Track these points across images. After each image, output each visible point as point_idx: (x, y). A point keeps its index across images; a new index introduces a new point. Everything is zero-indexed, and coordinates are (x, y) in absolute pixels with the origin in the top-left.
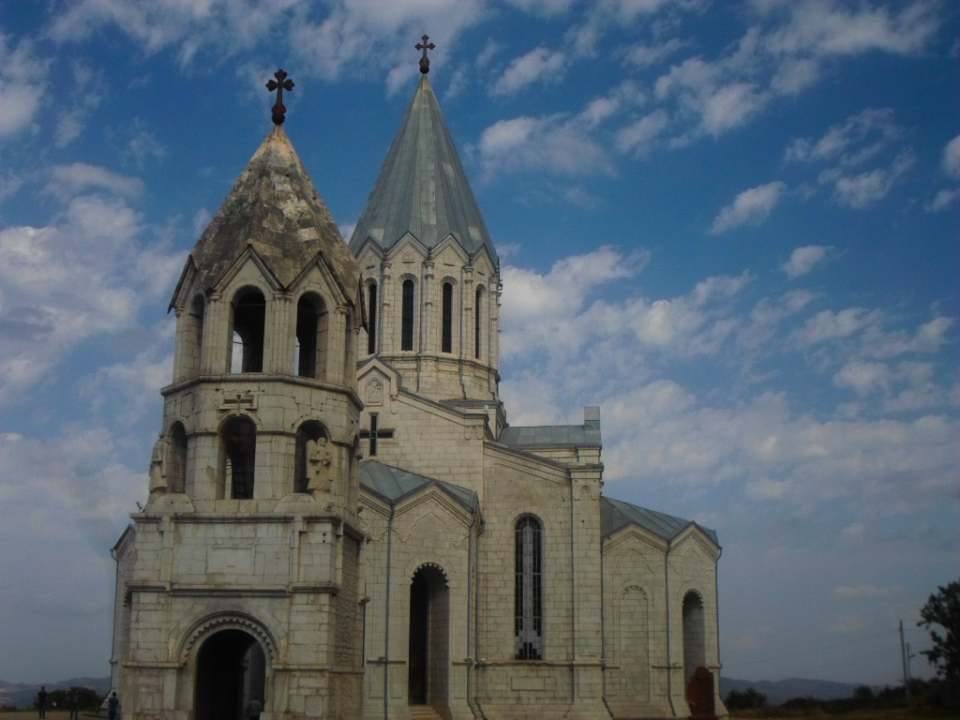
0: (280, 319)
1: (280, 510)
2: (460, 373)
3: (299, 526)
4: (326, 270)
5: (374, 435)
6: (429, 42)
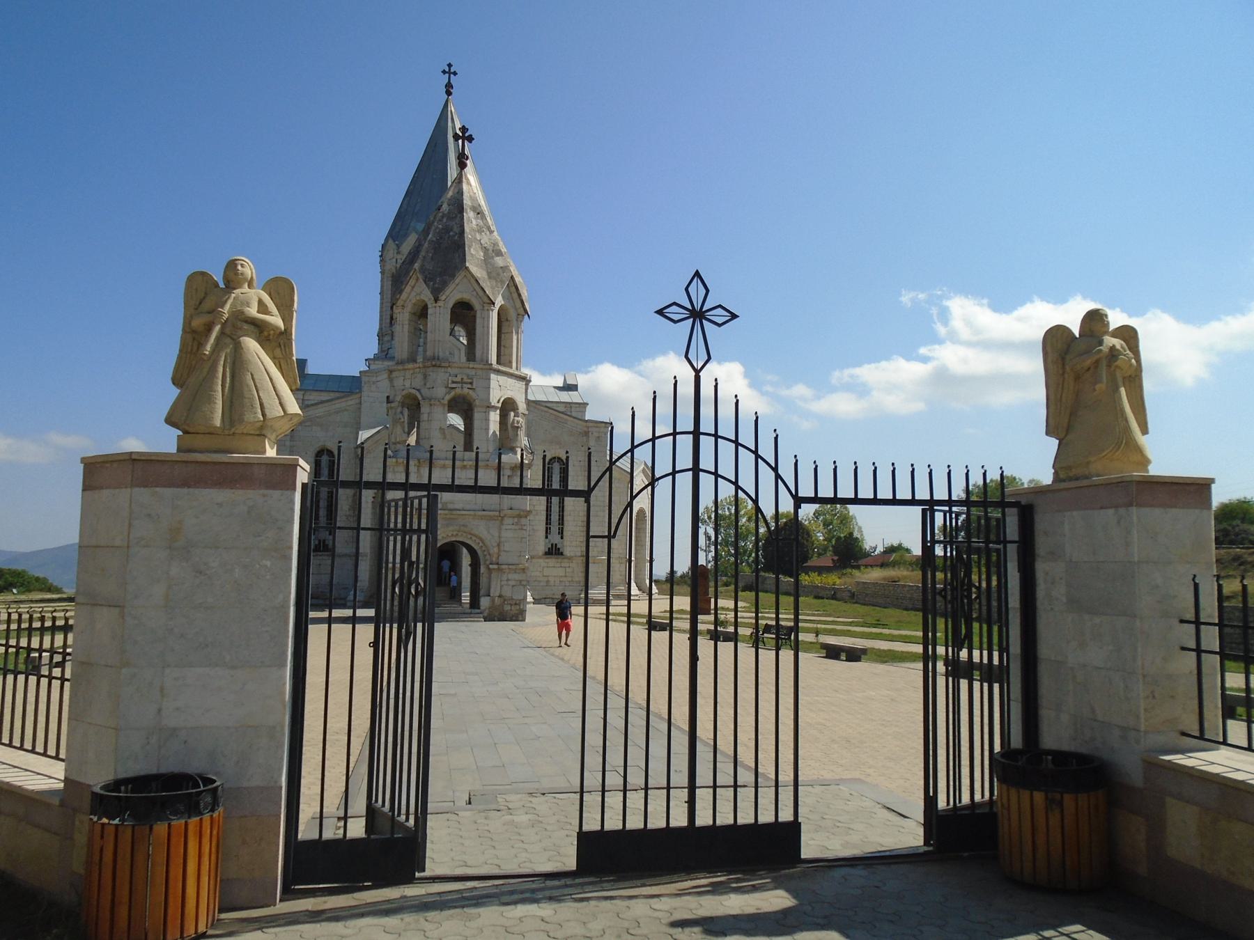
4: (513, 289)
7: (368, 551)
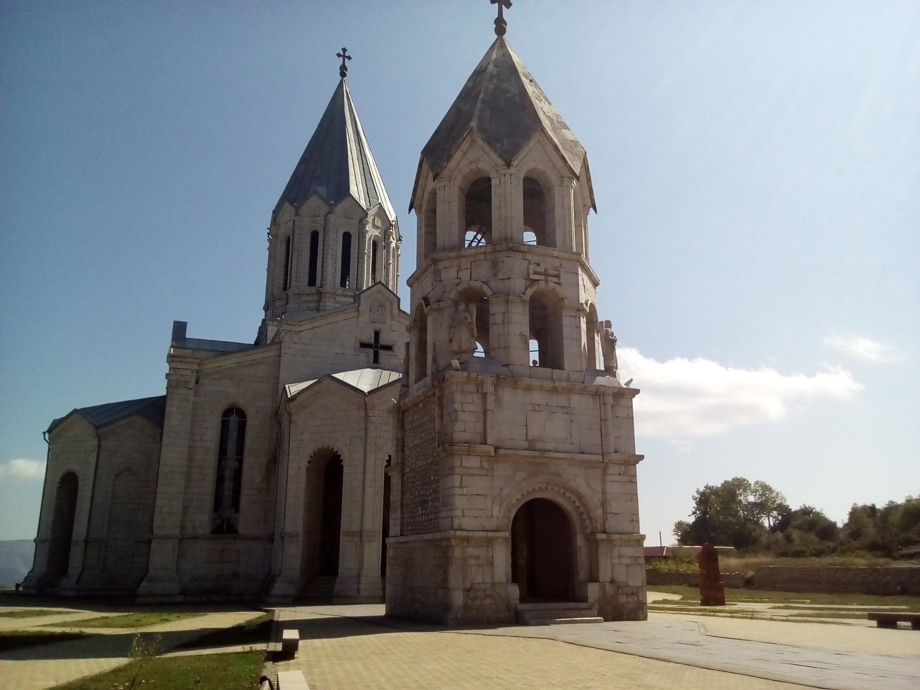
3: (610, 400)
5: (376, 347)
6: (347, 54)
7: (300, 529)
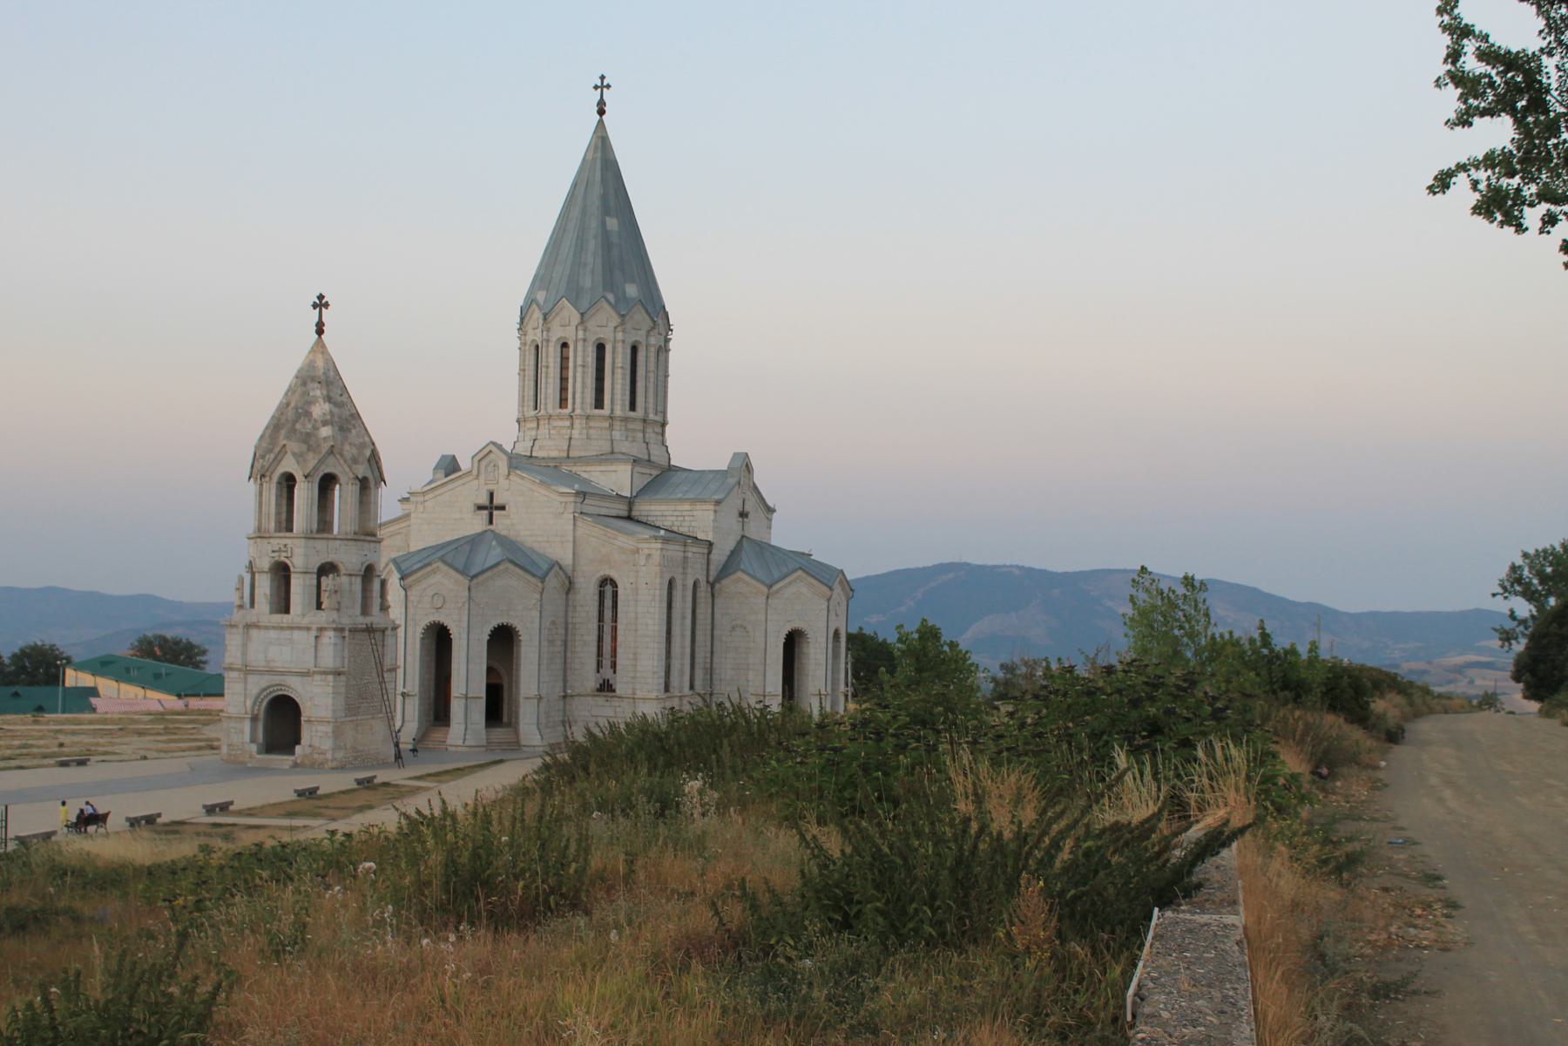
0: (304, 494)
1: (305, 621)
2: (611, 426)
3: (314, 633)
